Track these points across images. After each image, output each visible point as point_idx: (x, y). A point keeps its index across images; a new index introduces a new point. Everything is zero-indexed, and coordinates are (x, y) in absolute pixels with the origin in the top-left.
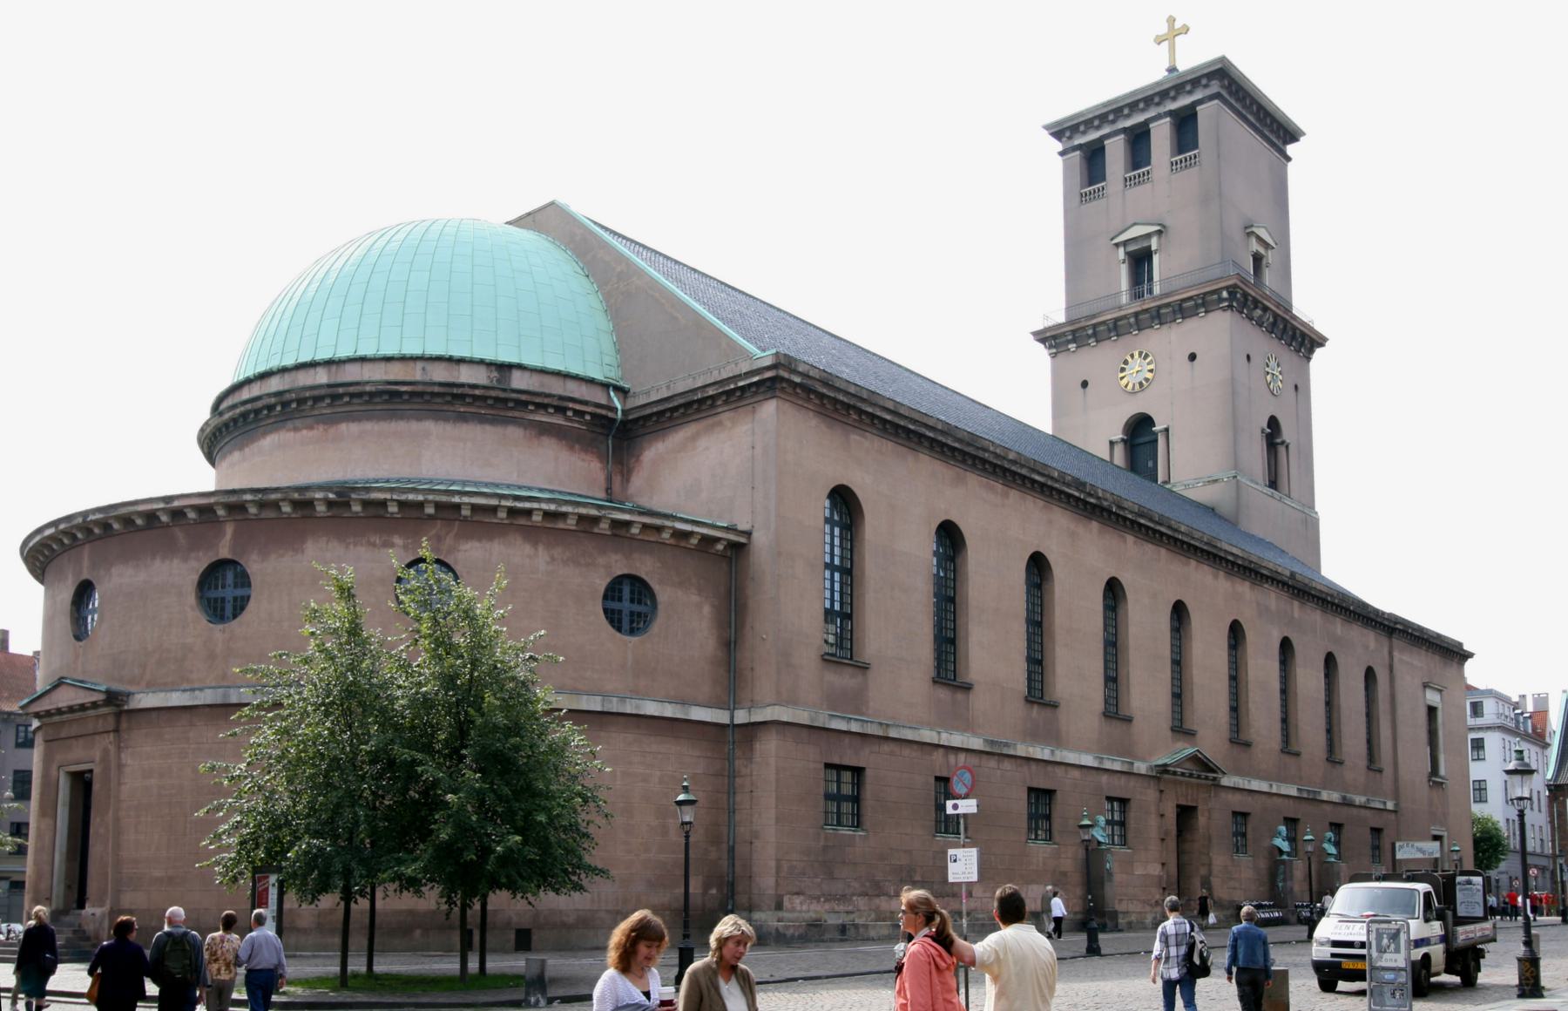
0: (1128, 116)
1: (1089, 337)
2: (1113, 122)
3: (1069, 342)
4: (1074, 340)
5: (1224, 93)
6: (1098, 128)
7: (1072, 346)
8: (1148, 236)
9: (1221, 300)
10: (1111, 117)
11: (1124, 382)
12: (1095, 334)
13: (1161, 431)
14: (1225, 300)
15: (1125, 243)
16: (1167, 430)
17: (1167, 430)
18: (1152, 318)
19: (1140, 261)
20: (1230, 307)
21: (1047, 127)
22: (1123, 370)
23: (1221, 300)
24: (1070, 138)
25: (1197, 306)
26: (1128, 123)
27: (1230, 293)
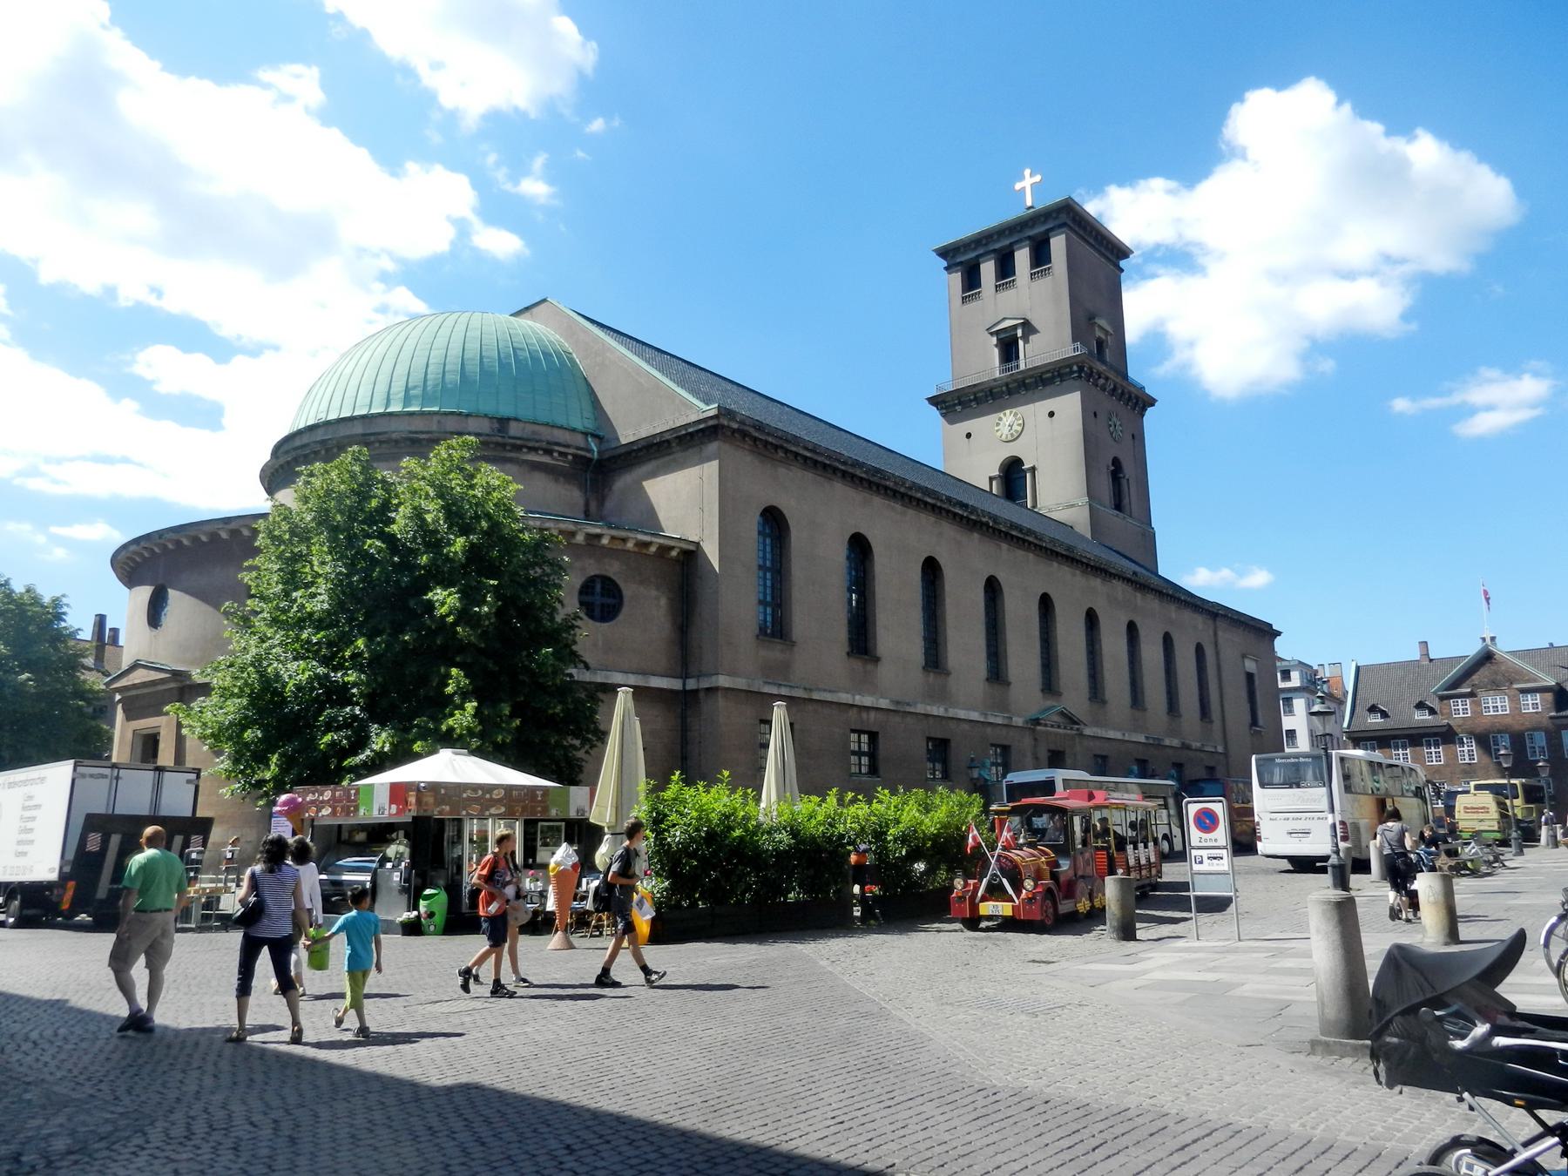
0: (998, 240)
1: (971, 401)
2: (986, 245)
3: (955, 405)
4: (960, 404)
5: (1069, 223)
6: (975, 249)
7: (959, 408)
8: (1015, 327)
9: (1073, 372)
10: (984, 242)
11: (999, 434)
12: (976, 399)
13: (1029, 469)
14: (1075, 372)
15: (997, 333)
16: (1033, 469)
17: (1033, 469)
18: (1019, 387)
19: (1008, 347)
20: (1080, 377)
21: (935, 251)
22: (998, 424)
23: (1072, 372)
24: (953, 257)
25: (1053, 377)
26: (997, 246)
27: (1078, 367)
